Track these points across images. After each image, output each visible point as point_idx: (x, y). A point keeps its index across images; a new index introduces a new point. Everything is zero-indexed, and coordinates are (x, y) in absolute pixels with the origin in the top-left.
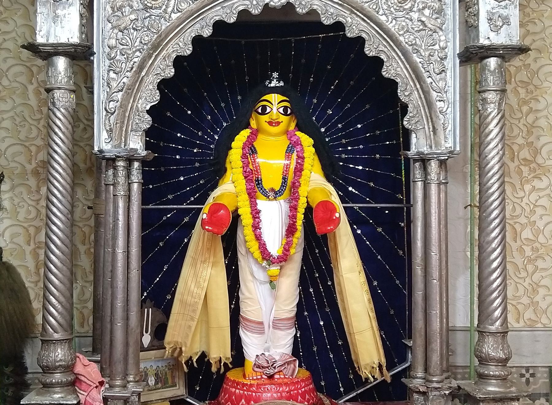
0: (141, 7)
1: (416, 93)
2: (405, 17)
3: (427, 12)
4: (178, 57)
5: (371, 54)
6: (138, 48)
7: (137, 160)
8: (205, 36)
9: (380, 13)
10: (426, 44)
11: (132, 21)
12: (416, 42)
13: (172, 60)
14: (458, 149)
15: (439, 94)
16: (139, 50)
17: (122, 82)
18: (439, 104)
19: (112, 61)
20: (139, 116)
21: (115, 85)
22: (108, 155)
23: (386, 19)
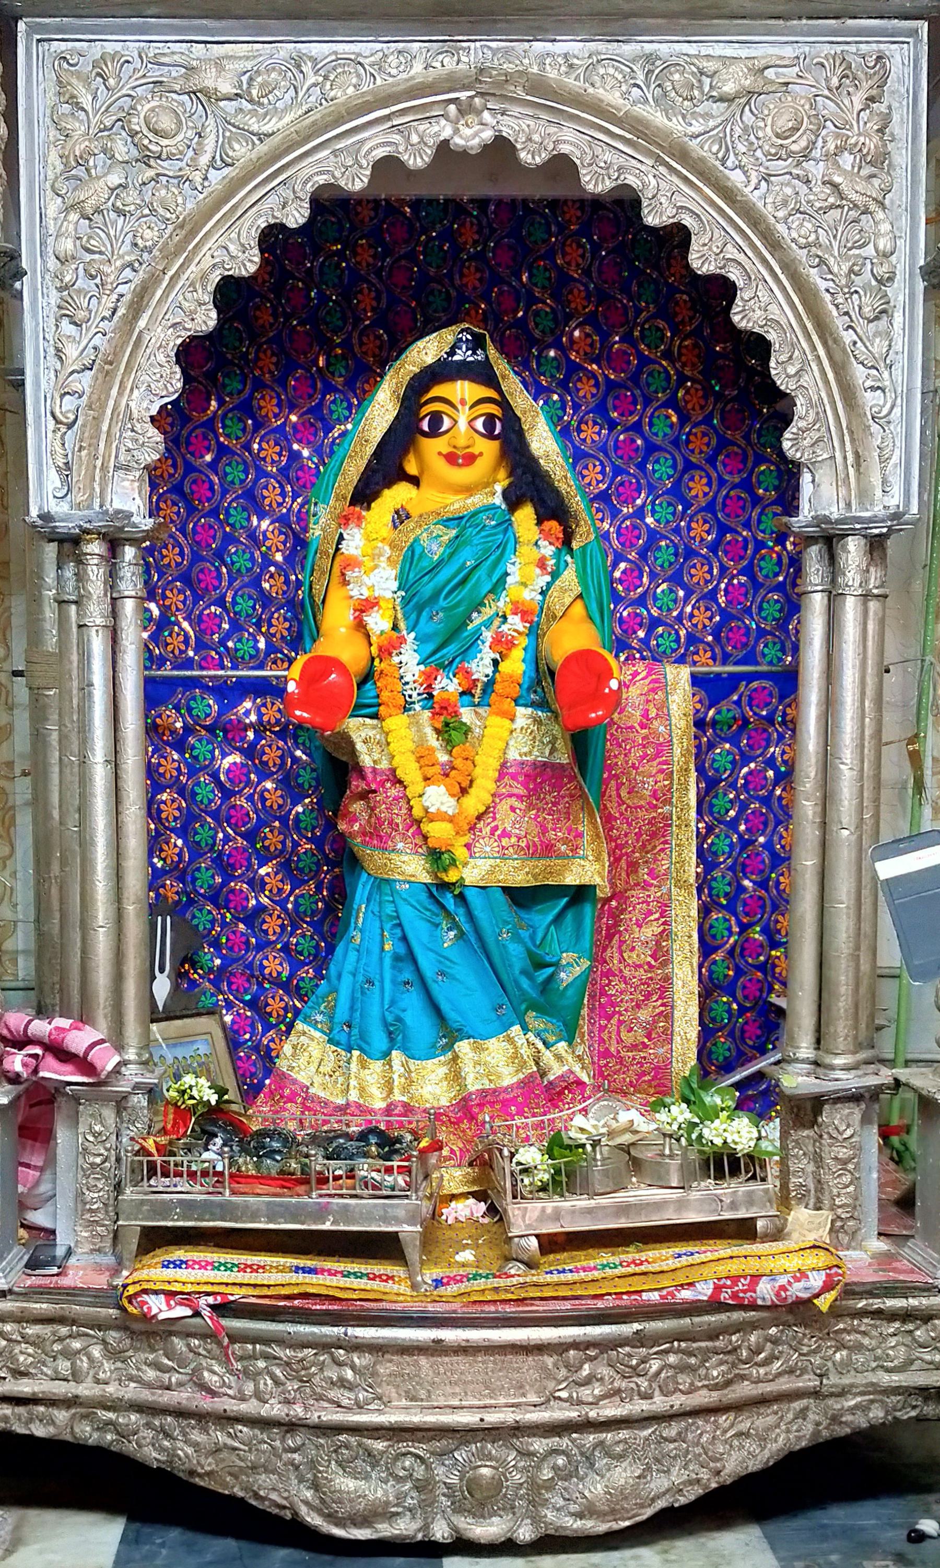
0: (135, 153)
1: (815, 368)
2: (791, 174)
3: (847, 160)
4: (224, 278)
5: (704, 269)
6: (127, 258)
7: (133, 541)
8: (292, 224)
9: (729, 164)
10: (843, 244)
11: (113, 190)
12: (818, 239)
13: (211, 288)
14: (914, 509)
15: (874, 372)
16: (130, 265)
17: (91, 345)
18: (871, 400)
19: (66, 293)
20: (133, 431)
21: (76, 354)
22: (63, 527)
23: (744, 178)
